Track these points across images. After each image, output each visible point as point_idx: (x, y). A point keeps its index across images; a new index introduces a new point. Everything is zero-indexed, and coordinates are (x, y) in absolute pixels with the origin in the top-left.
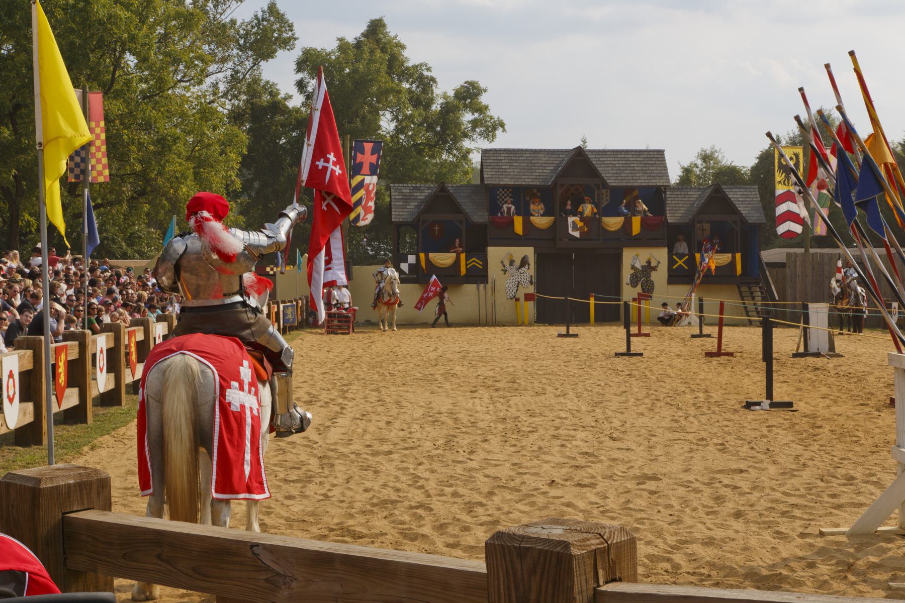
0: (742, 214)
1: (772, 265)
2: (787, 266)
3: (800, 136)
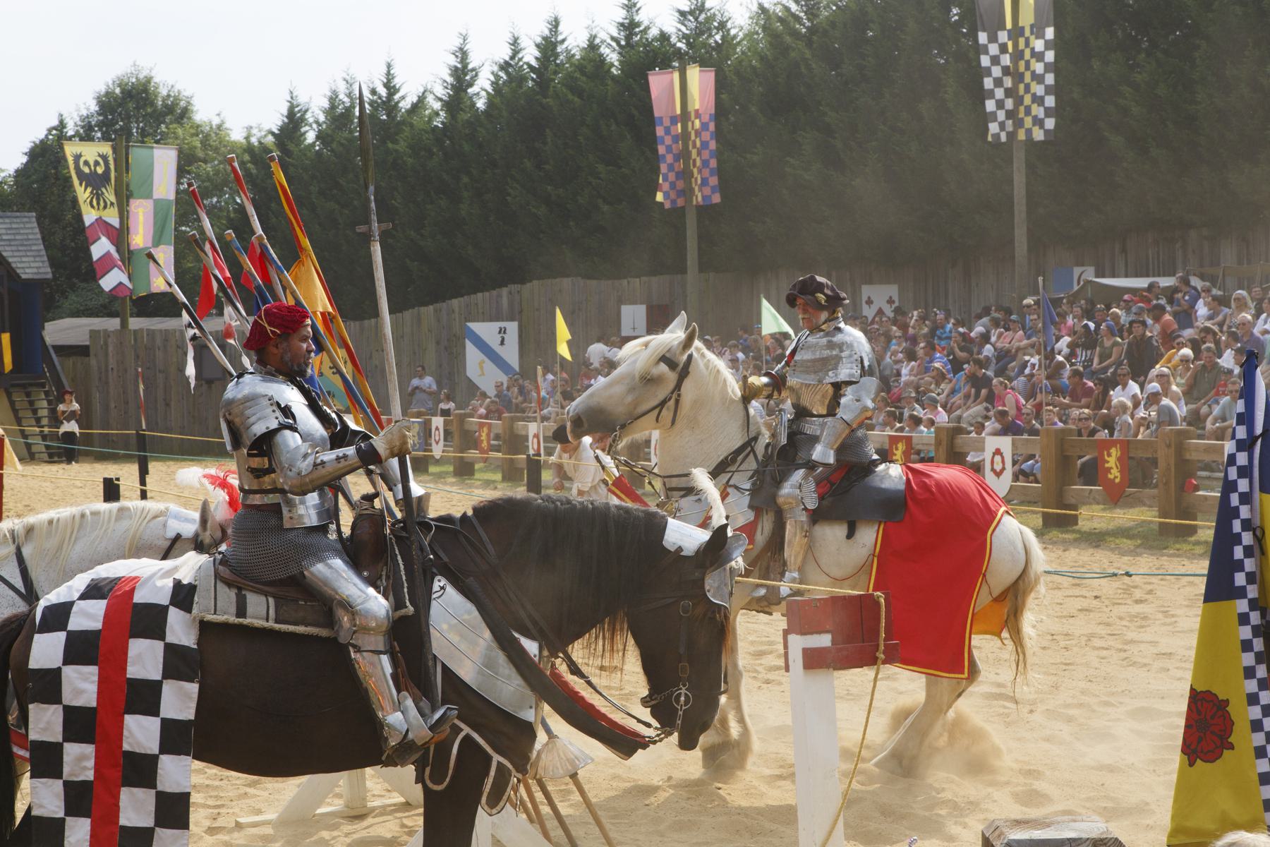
0: (9, 264)
1: (63, 350)
2: (92, 351)
3: (99, 114)
